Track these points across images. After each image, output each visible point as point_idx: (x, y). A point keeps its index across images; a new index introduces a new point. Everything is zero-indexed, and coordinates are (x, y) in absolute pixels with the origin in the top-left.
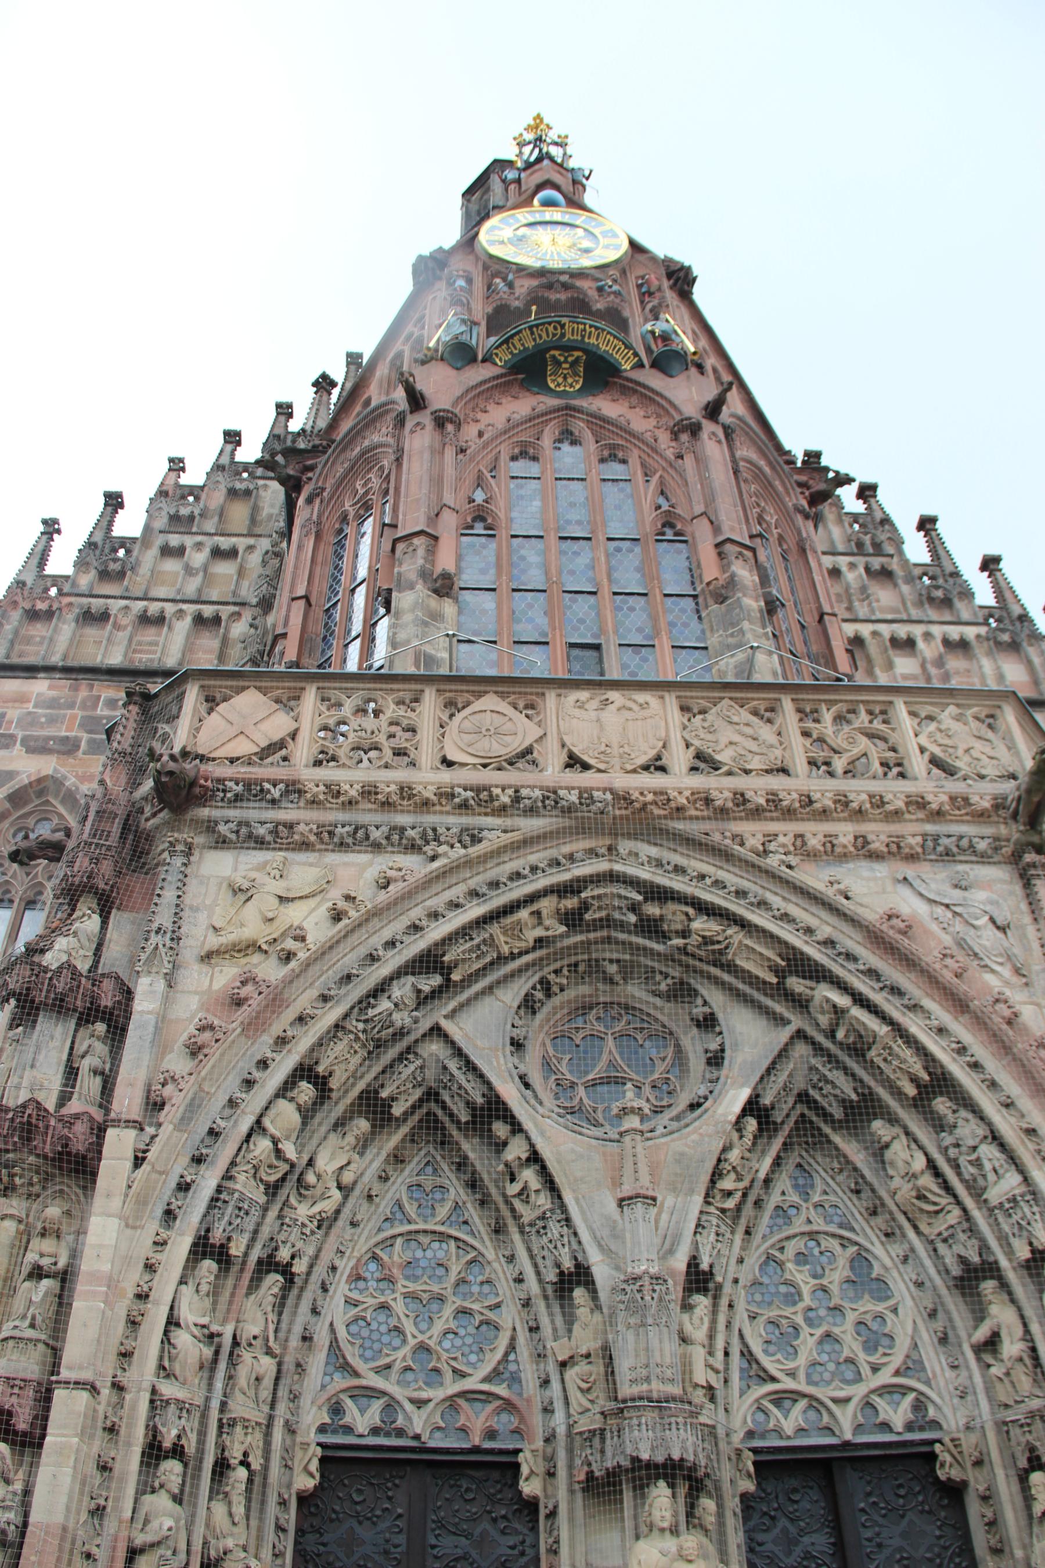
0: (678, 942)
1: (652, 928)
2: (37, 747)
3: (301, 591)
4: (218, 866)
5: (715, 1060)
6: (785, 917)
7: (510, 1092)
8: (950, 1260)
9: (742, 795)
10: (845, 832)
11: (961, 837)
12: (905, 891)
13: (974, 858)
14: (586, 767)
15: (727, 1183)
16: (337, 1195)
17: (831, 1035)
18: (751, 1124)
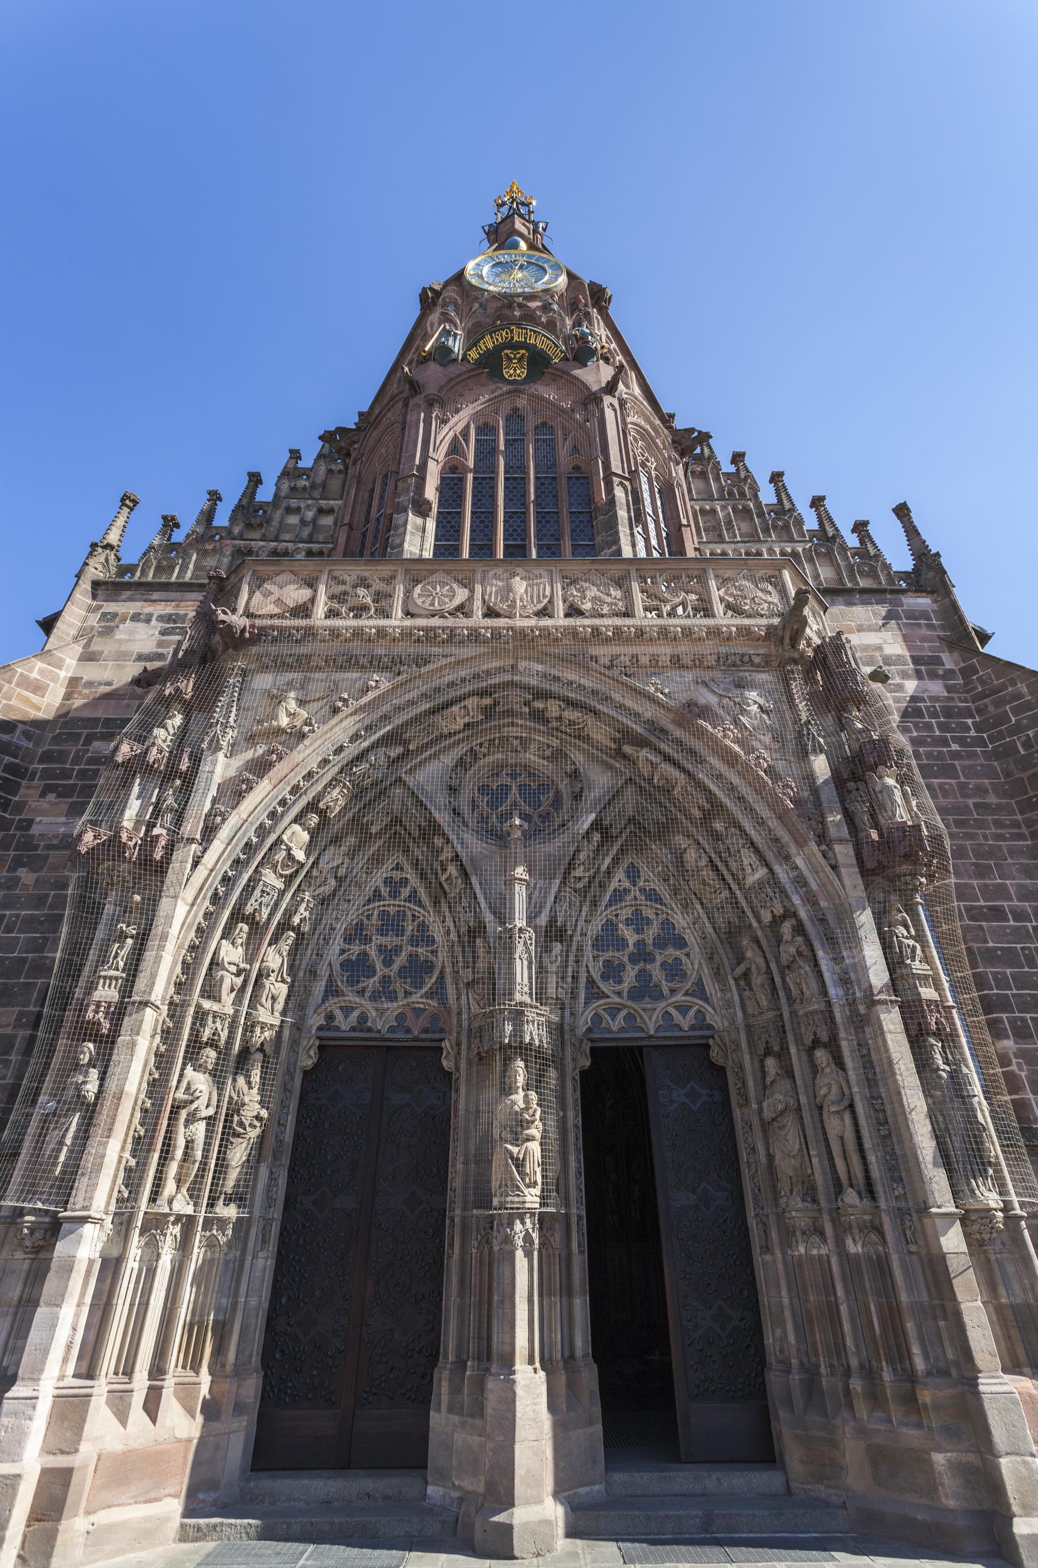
0: (555, 724)
1: (539, 716)
3: (346, 521)
4: (264, 681)
5: (577, 797)
6: (621, 707)
7: (443, 818)
8: (720, 921)
9: (597, 630)
10: (664, 651)
11: (743, 655)
12: (704, 691)
13: (751, 668)
14: (498, 615)
15: (579, 872)
16: (333, 883)
17: (650, 781)
18: (596, 837)
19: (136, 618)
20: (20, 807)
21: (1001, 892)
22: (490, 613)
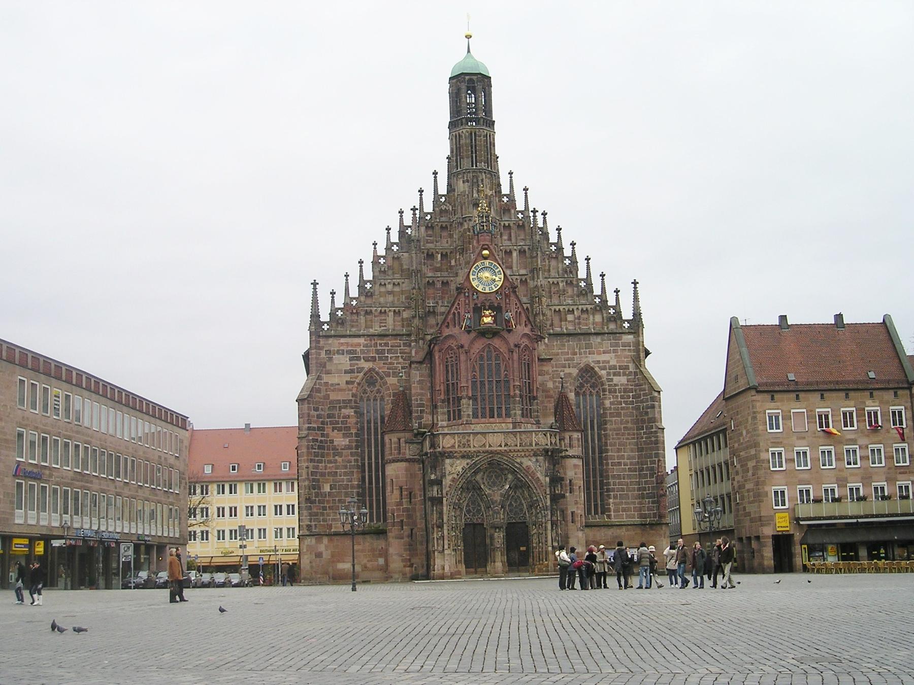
2: (367, 360)
4: (448, 461)
10: (523, 454)
19: (338, 352)
20: (328, 435)
21: (622, 457)
22: (490, 446)
